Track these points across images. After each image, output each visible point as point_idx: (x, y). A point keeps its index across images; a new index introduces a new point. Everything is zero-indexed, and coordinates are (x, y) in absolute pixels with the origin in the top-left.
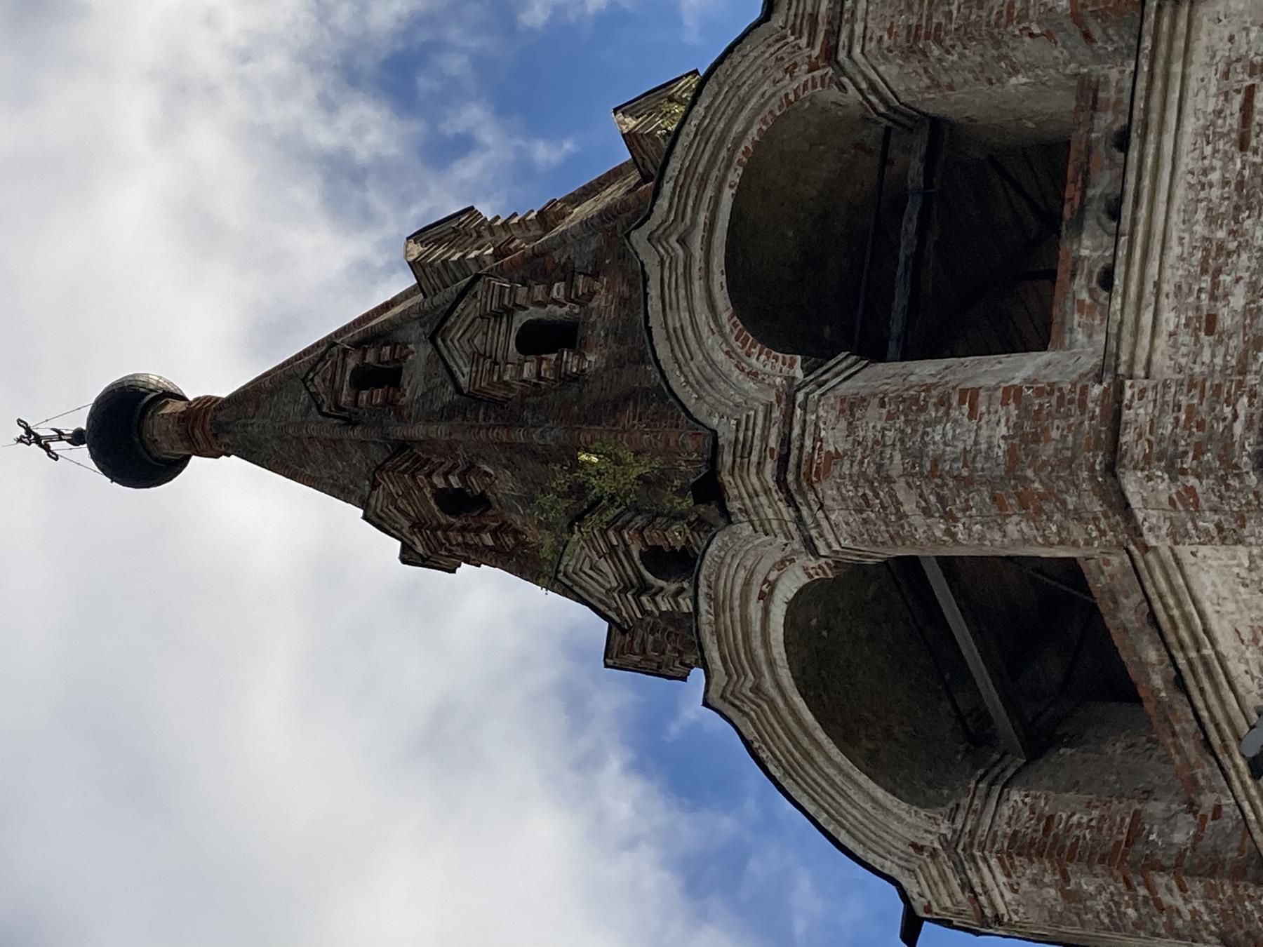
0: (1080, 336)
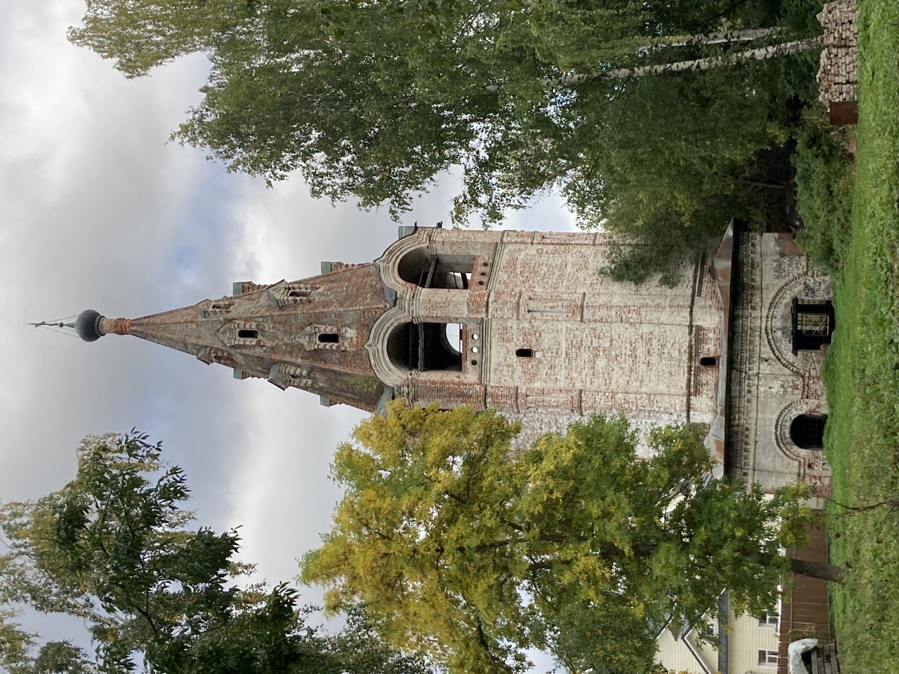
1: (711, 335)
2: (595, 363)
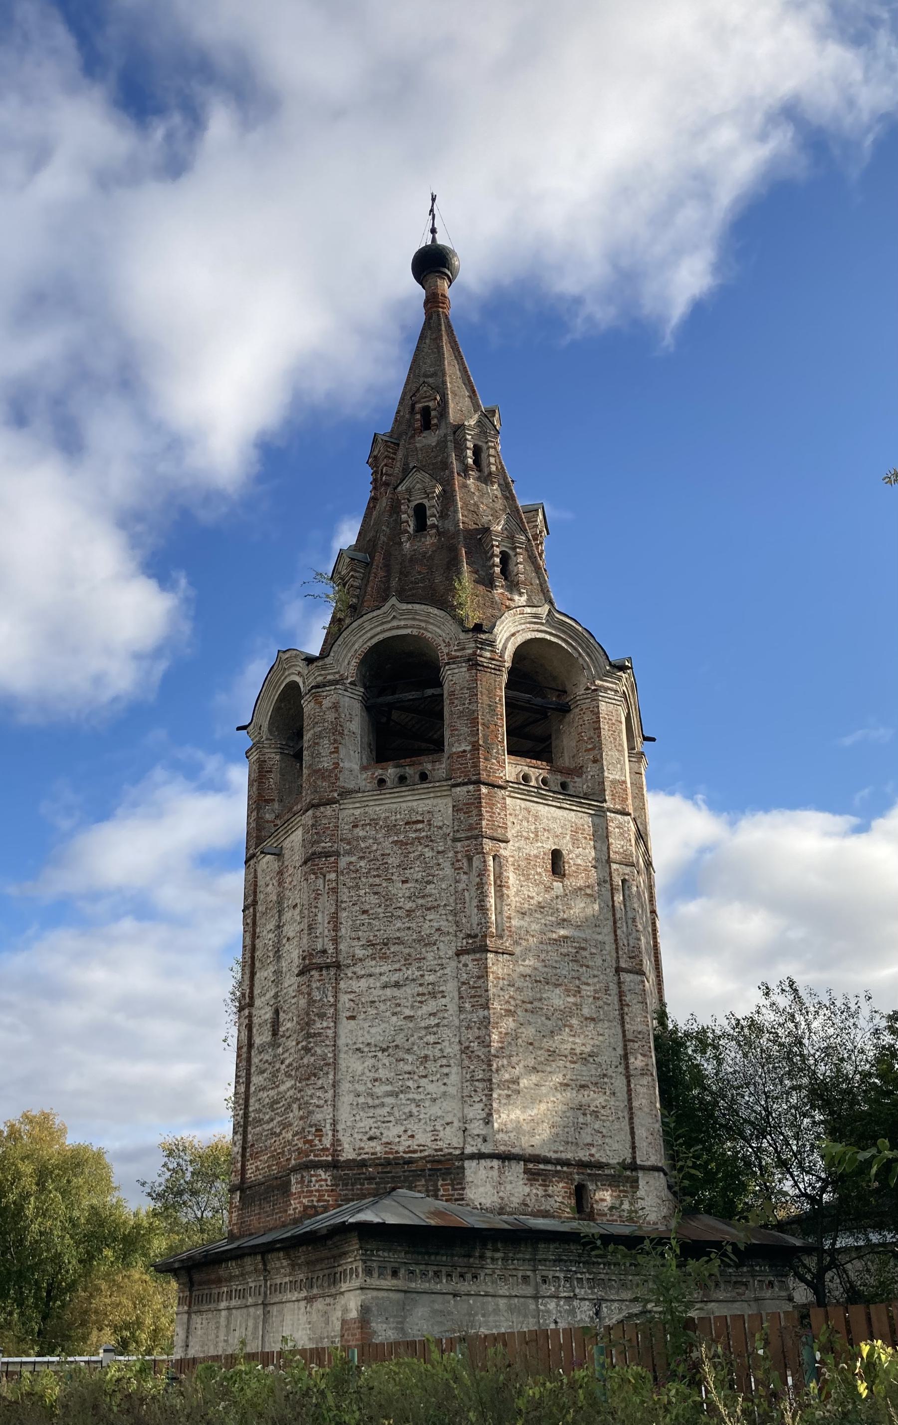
0: (364, 776)
2: (557, 985)
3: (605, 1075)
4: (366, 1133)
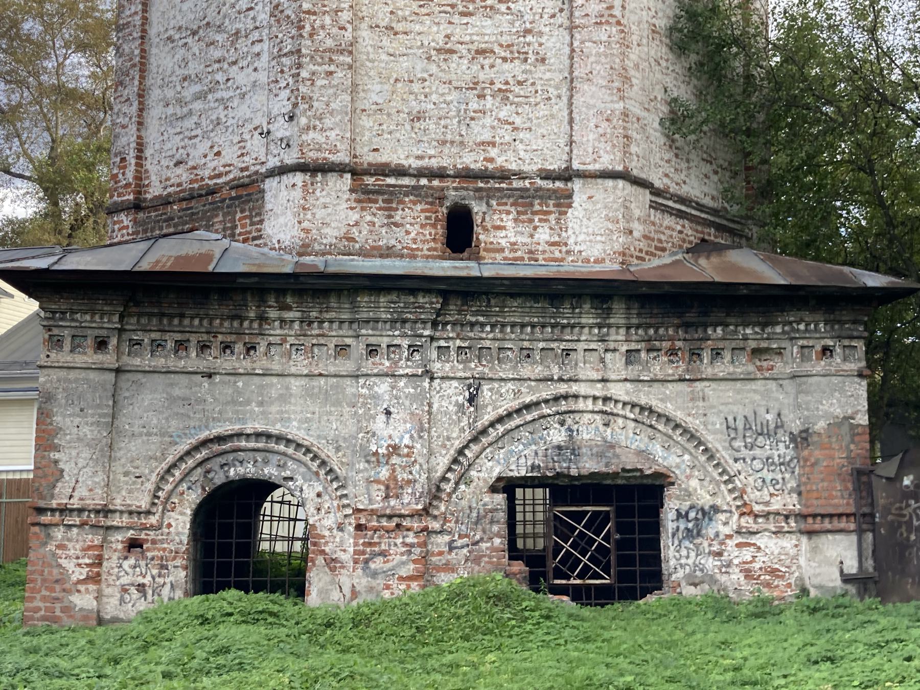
1: (543, 235)
3: (528, 32)
4: (173, 156)
